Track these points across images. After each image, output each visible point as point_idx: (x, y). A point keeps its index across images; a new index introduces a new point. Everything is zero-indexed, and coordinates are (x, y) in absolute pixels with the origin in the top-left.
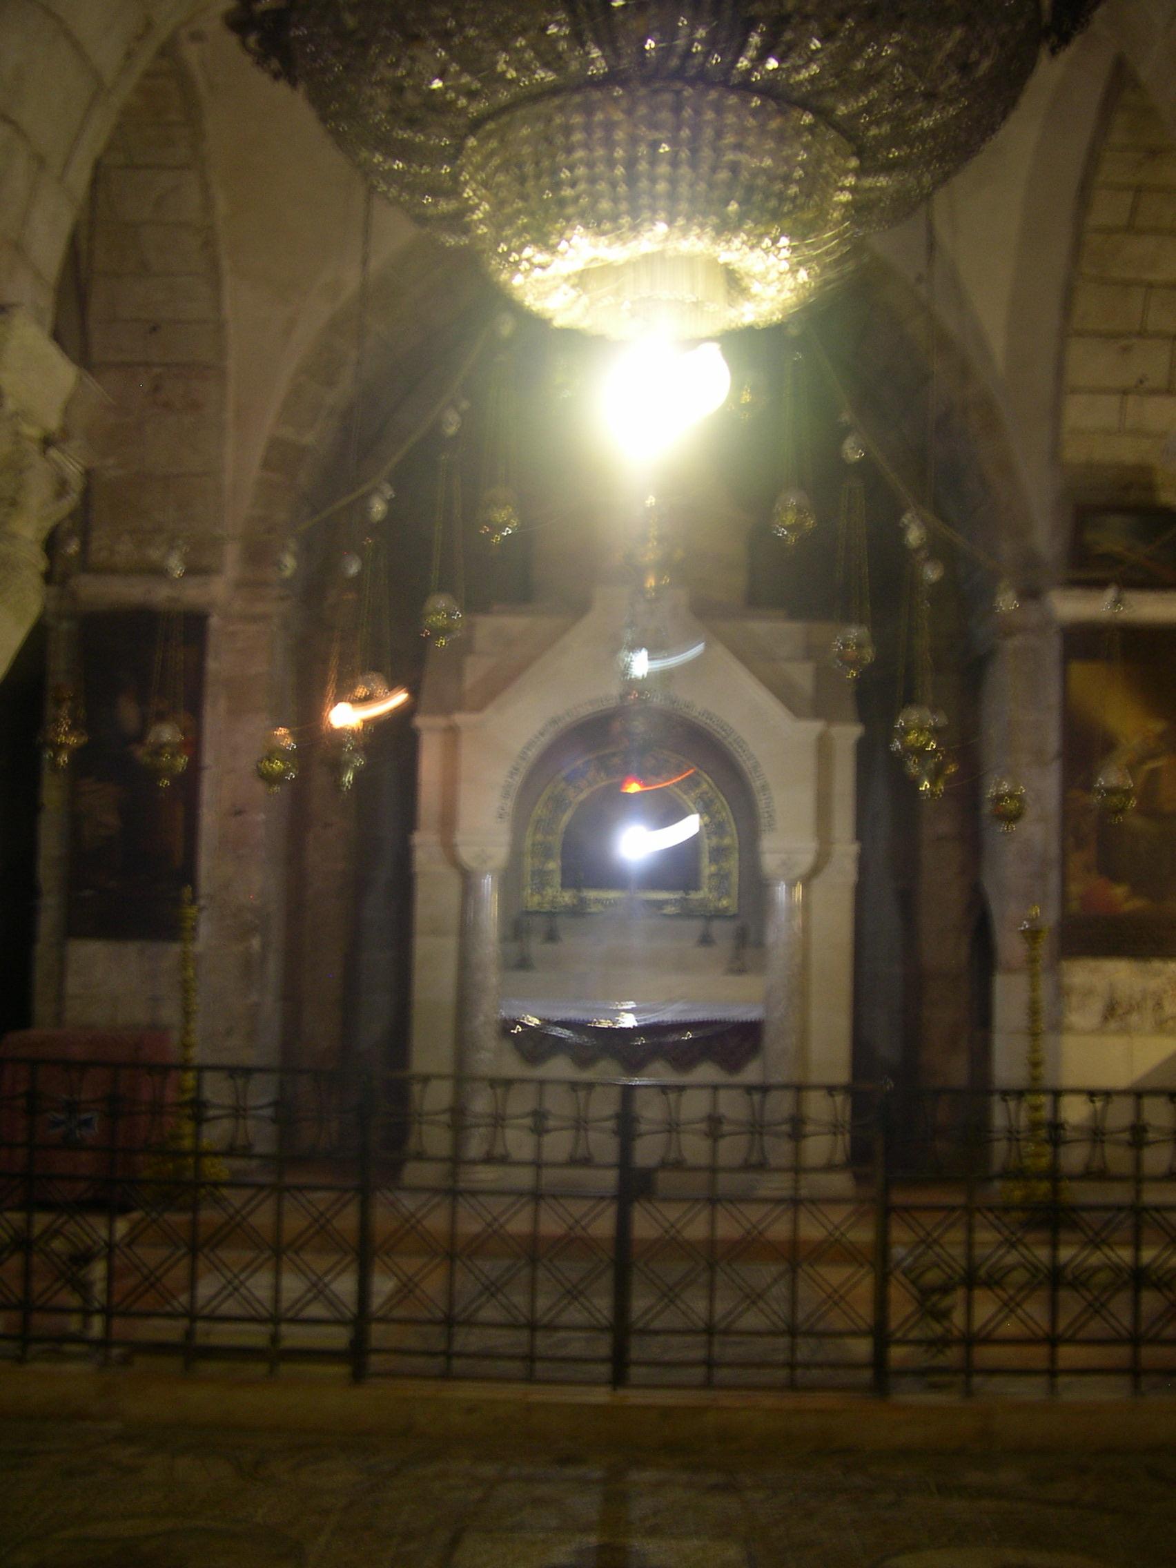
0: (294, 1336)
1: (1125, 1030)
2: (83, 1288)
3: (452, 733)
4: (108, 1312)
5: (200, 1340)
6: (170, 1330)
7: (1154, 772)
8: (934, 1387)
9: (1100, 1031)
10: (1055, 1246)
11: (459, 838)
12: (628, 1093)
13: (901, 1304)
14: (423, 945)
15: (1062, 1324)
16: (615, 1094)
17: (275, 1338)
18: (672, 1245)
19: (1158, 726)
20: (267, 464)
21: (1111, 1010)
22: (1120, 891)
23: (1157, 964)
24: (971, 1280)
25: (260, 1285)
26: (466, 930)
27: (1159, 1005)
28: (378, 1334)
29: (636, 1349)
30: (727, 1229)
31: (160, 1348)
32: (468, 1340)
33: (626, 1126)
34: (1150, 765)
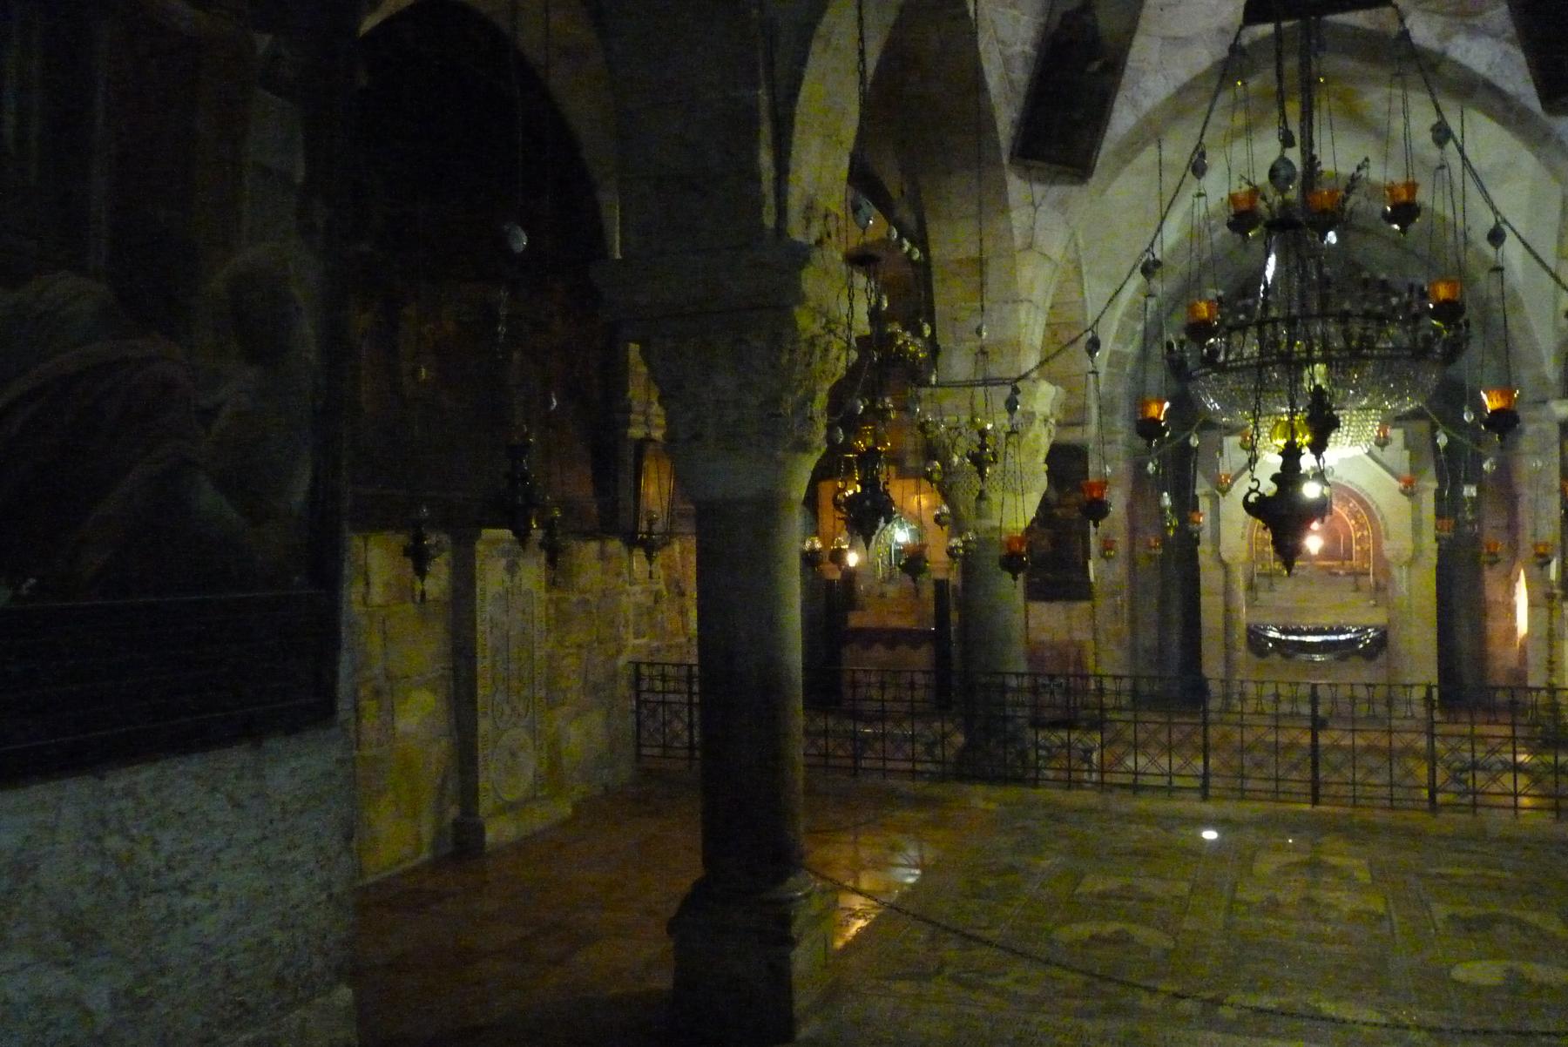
0: (1177, 782)
2: (1089, 762)
4: (1102, 772)
5: (1139, 782)
6: (1127, 779)
8: (1459, 812)
10: (1515, 753)
11: (1223, 548)
12: (1314, 687)
13: (1441, 776)
14: (1205, 600)
15: (1520, 788)
16: (1309, 687)
17: (1170, 783)
18: (1335, 747)
24: (1475, 766)
25: (1164, 761)
26: (1228, 591)
28: (1213, 781)
29: (1322, 791)
30: (1360, 742)
31: (1123, 786)
32: (1250, 784)
33: (1314, 700)
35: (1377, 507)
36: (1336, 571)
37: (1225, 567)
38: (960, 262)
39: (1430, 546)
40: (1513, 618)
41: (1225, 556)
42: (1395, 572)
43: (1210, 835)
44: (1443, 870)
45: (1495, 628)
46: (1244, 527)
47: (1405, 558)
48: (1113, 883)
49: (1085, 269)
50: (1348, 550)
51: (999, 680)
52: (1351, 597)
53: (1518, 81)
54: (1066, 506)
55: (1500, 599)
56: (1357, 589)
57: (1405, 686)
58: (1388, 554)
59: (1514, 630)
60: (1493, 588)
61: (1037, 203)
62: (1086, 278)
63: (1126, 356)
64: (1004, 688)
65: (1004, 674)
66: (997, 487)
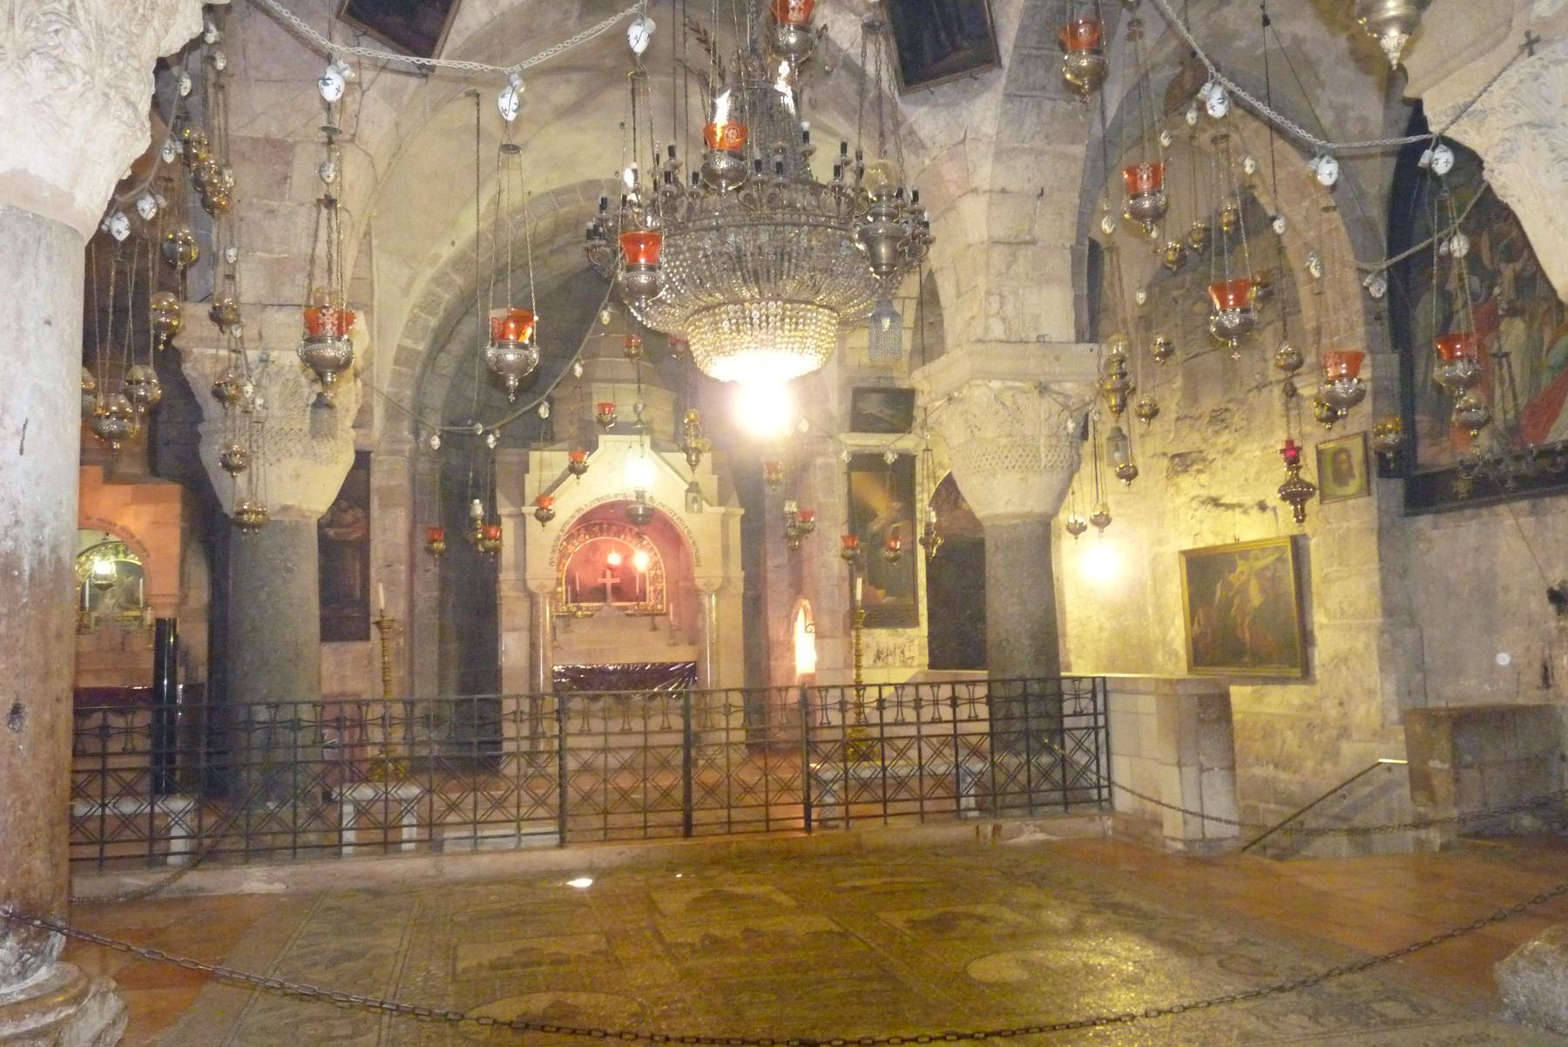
1: (886, 666)
7: (897, 528)
11: (529, 574)
19: (897, 505)
20: (397, 361)
21: (878, 657)
22: (881, 593)
23: (900, 630)
27: (903, 652)
34: (894, 526)
35: (689, 532)
37: (532, 598)
38: (255, 142)
39: (737, 573)
40: (793, 660)
41: (532, 585)
42: (705, 600)
43: (583, 883)
44: (859, 883)
46: (553, 551)
47: (716, 586)
48: (505, 950)
49: (375, 242)
50: (643, 591)
51: (287, 714)
52: (650, 636)
53: (879, 63)
54: (341, 526)
56: (654, 628)
57: (779, 689)
58: (699, 583)
60: (776, 631)
61: (365, 86)
62: (375, 253)
63: (419, 353)
64: (295, 725)
65: (296, 704)
66: (293, 450)
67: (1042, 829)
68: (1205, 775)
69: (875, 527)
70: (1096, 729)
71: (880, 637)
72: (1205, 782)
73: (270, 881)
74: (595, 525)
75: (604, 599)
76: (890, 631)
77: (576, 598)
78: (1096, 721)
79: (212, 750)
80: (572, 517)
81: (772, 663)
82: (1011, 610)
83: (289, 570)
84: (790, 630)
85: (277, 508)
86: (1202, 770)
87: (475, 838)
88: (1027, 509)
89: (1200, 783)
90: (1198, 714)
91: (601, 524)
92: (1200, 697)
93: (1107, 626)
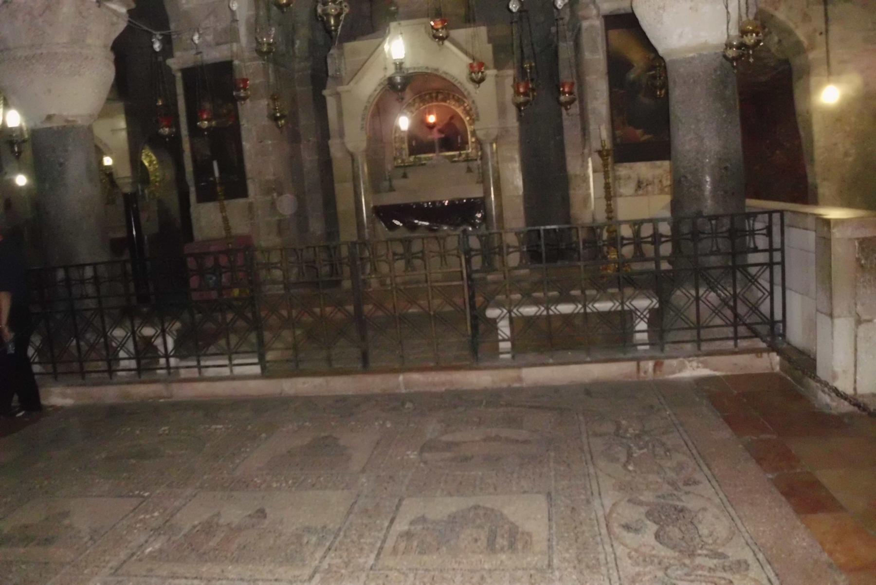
1: (647, 193)
3: (338, 95)
9: (636, 194)
14: (338, 187)
21: (639, 185)
22: (639, 132)
23: (658, 163)
27: (661, 181)
36: (456, 159)
37: (352, 157)
41: (350, 146)
45: (575, 195)
46: (363, 119)
55: (578, 173)
59: (589, 195)
67: (706, 366)
68: (862, 328)
69: (632, 76)
70: (771, 265)
71: (644, 169)
72: (861, 334)
73: (65, 396)
74: (425, 95)
75: (434, 152)
76: (649, 163)
77: (413, 151)
78: (771, 257)
79: (317, 249)
80: (375, 90)
81: (572, 192)
82: (687, 147)
83: (61, 164)
84: (584, 166)
85: (45, 117)
86: (859, 322)
87: (199, 367)
88: (703, 40)
89: (856, 336)
90: (858, 260)
91: (430, 94)
92: (863, 242)
93: (853, 151)
